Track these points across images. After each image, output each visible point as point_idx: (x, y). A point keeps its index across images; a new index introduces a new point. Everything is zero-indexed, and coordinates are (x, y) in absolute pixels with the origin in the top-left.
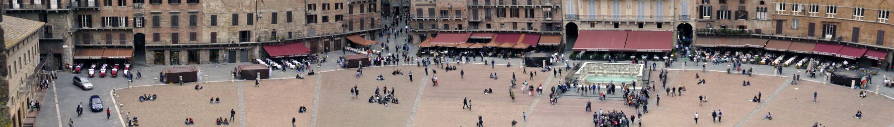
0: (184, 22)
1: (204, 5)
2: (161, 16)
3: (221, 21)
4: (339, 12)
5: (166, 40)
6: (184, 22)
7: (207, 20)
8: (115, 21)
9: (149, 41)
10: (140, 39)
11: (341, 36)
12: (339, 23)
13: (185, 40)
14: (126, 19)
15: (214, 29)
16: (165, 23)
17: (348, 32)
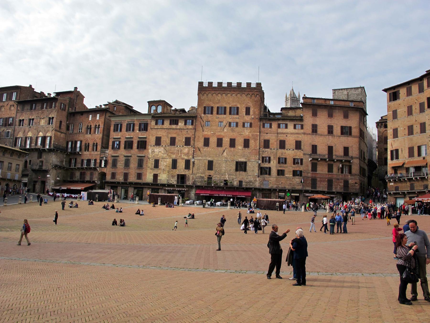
0: (134, 164)
1: (150, 151)
2: (119, 159)
3: (163, 164)
4: (298, 168)
5: (120, 178)
6: (134, 164)
7: (151, 164)
8: (89, 161)
9: (108, 178)
10: (103, 175)
11: (299, 191)
12: (297, 180)
13: (132, 178)
14: (95, 160)
15: (156, 171)
16: (121, 164)
17: (309, 188)
